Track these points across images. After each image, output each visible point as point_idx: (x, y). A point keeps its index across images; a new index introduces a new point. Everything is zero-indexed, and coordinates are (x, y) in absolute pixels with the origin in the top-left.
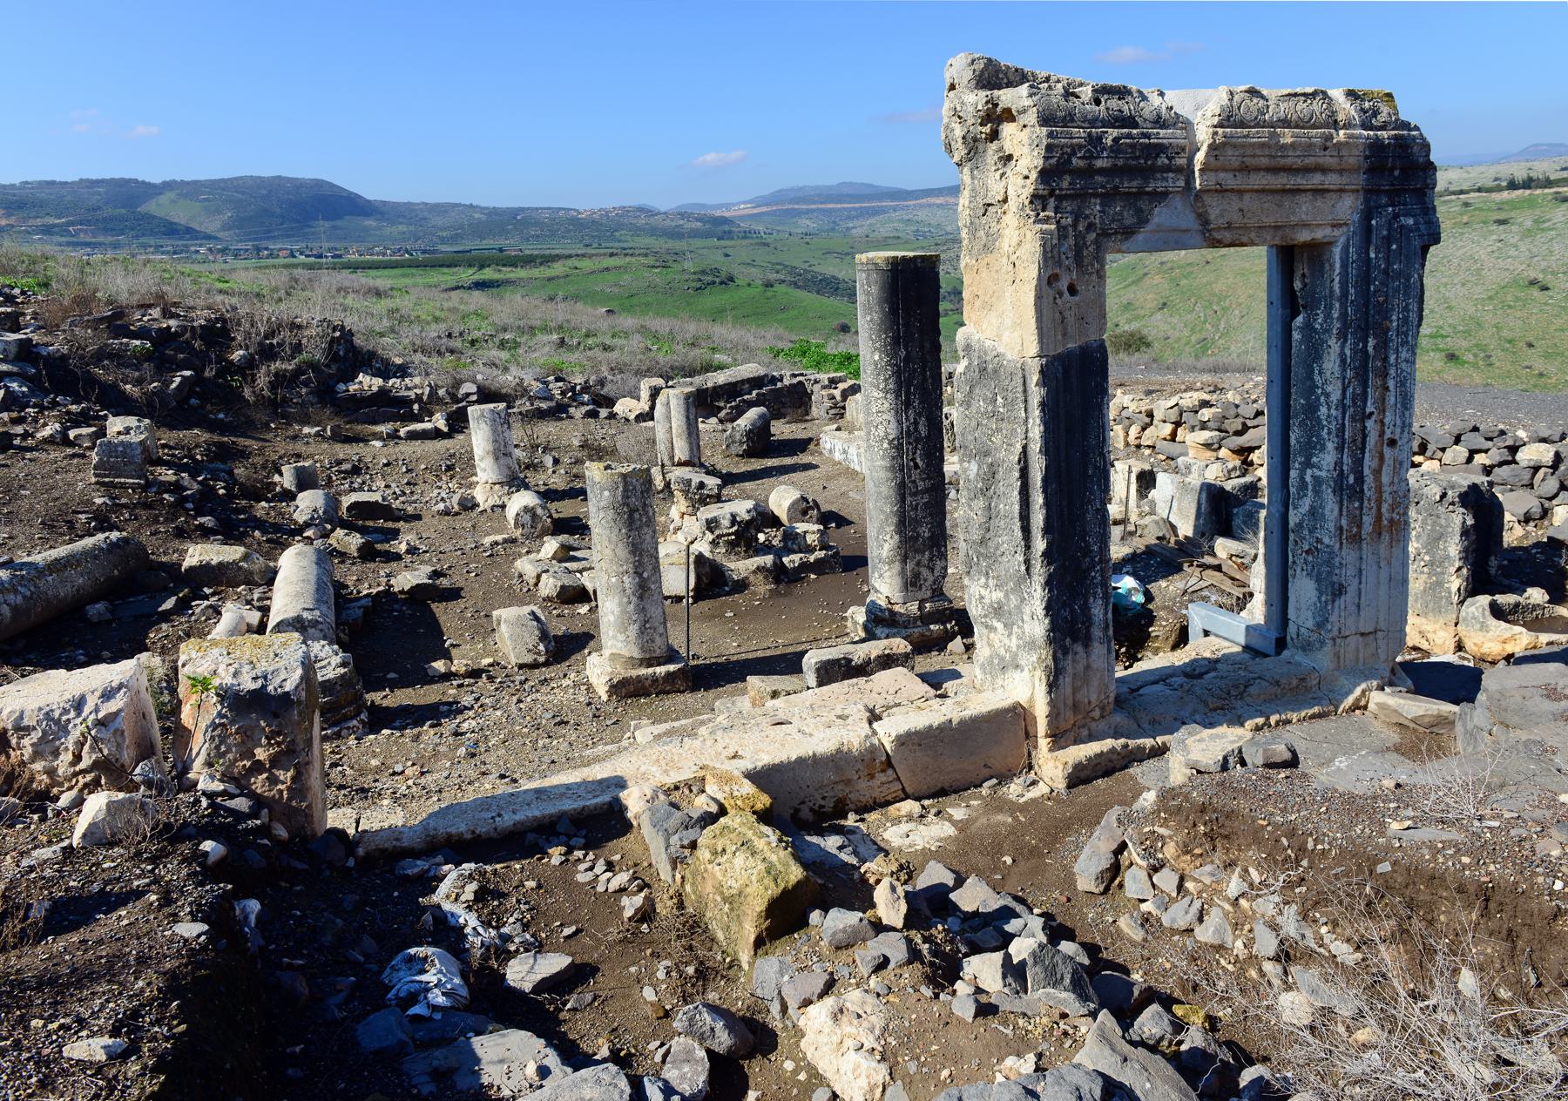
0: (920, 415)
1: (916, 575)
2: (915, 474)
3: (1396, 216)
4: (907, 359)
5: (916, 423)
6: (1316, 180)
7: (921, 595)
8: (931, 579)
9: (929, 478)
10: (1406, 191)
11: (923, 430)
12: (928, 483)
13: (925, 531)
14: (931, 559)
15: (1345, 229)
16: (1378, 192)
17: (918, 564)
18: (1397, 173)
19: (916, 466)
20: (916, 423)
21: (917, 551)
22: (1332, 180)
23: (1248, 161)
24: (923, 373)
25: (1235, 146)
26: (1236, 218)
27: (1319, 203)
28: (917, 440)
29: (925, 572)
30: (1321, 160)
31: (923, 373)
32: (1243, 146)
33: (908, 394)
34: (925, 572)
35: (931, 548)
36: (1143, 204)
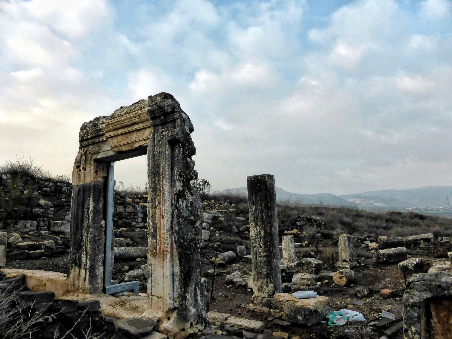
0: (261, 229)
1: (262, 287)
2: (260, 250)
3: (163, 132)
4: (256, 209)
5: (260, 232)
6: (136, 127)
7: (263, 295)
8: (267, 290)
9: (265, 252)
10: (168, 122)
11: (263, 234)
12: (265, 254)
13: (264, 271)
14: (267, 282)
15: (149, 140)
16: (158, 125)
17: (262, 283)
18: (162, 117)
19: (261, 247)
20: (260, 232)
21: (261, 278)
22: (140, 126)
23: (116, 127)
24: (262, 214)
25: (111, 124)
26: (116, 144)
27: (139, 134)
28: (260, 238)
29: (265, 287)
30: (134, 121)
31: (262, 214)
32: (113, 123)
33: (257, 221)
34: (265, 287)
35: (267, 278)
36: (100, 145)
